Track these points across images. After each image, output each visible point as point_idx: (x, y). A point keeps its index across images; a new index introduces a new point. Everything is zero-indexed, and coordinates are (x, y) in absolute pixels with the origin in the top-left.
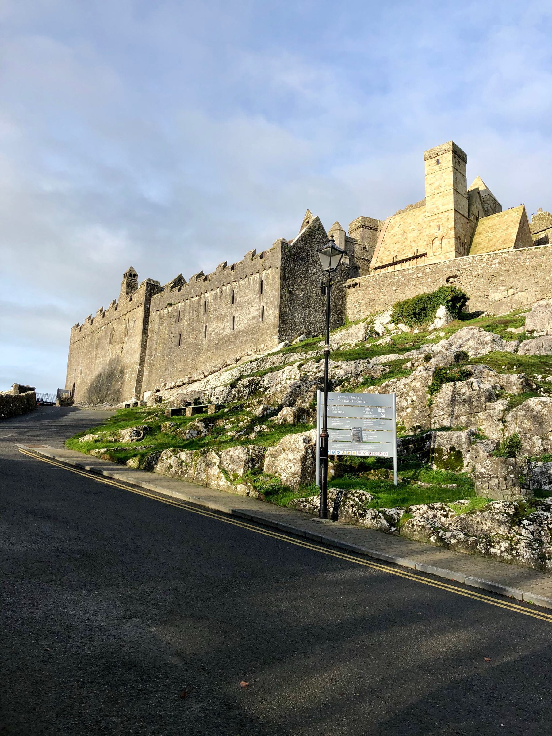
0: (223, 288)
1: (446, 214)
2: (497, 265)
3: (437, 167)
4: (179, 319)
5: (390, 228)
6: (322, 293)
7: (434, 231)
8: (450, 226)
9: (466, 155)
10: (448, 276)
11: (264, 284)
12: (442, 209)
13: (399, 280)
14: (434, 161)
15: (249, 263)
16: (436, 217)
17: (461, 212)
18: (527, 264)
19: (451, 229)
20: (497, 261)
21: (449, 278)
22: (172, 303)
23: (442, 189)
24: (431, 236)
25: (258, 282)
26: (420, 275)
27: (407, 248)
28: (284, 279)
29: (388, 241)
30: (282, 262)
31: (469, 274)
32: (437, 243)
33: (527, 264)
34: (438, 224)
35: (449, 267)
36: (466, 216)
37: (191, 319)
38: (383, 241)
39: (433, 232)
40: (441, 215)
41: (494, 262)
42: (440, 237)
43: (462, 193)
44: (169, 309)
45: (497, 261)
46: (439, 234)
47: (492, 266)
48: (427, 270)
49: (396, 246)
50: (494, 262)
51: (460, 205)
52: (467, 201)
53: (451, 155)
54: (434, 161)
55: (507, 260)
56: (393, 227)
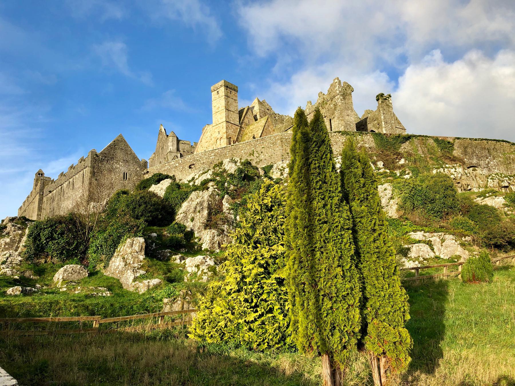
0: (70, 180)
1: (222, 124)
2: (213, 157)
3: (217, 96)
4: (54, 200)
5: (206, 133)
6: (124, 179)
7: (216, 135)
8: (224, 132)
9: (237, 87)
10: (189, 164)
11: (85, 176)
12: (220, 121)
13: (167, 168)
14: (216, 92)
15: (80, 164)
16: (217, 126)
17: (233, 123)
20: (213, 154)
21: (191, 165)
22: (52, 190)
23: (220, 109)
24: (215, 138)
25: (82, 176)
26: (177, 165)
27: (210, 145)
28: (93, 174)
29: (203, 141)
30: (91, 164)
31: (199, 163)
33: (227, 155)
34: (218, 130)
35: (191, 160)
36: (237, 124)
37: (58, 200)
38: (201, 141)
39: (216, 135)
40: (219, 125)
41: (212, 155)
42: (219, 138)
43: (234, 111)
44: (50, 194)
45: (213, 154)
47: (211, 157)
48: (181, 162)
49: (207, 144)
50: (212, 155)
51: (231, 118)
52: (238, 115)
53: (224, 88)
54: (216, 92)
55: (218, 153)
56: (207, 132)
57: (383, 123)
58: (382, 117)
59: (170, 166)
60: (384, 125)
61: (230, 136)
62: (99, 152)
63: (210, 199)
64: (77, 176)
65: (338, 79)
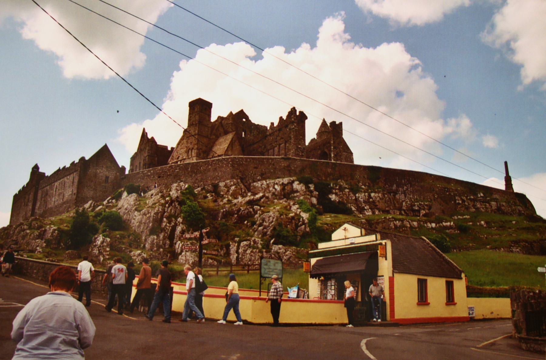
13: (141, 176)
18: (189, 170)
19: (195, 144)
26: (149, 174)
32: (190, 152)
34: (191, 141)
42: (191, 149)
46: (191, 146)
47: (176, 171)
48: (152, 172)
55: (182, 167)
57: (332, 147)
58: (332, 142)
59: (143, 174)
60: (332, 149)
61: (200, 147)
62: (87, 158)
63: (155, 215)
64: (68, 177)
65: (294, 108)
